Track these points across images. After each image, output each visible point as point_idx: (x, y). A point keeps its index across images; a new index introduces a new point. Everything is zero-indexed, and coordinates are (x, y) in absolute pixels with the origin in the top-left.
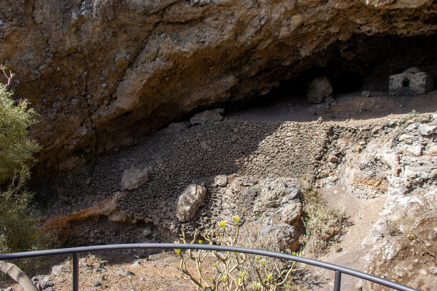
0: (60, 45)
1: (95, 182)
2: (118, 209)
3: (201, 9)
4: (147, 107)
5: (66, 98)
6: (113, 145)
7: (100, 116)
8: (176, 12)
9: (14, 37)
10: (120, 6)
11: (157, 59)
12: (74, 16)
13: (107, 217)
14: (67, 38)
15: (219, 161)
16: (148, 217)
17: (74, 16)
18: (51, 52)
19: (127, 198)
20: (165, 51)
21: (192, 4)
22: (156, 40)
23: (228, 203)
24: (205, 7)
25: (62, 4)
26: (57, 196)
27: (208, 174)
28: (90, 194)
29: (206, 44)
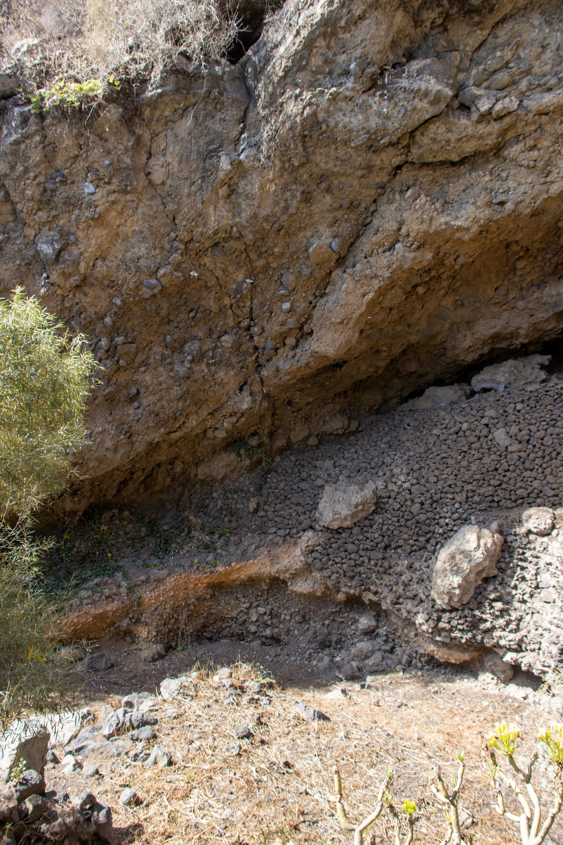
0: (197, 226)
1: (266, 507)
2: (308, 568)
3: (495, 127)
4: (378, 352)
5: (210, 332)
6: (307, 432)
7: (278, 370)
8: (439, 138)
9: (114, 214)
10: (315, 135)
11: (398, 246)
12: (225, 164)
13: (284, 582)
14: (211, 210)
15: (534, 474)
16: (369, 590)
17: (225, 164)
18: (181, 241)
19: (327, 546)
20: (415, 227)
21: (475, 116)
22: (395, 205)
23: (554, 575)
24: (507, 120)
25: (202, 142)
26: (189, 532)
27: (509, 504)
28: (254, 531)
29: (509, 206)
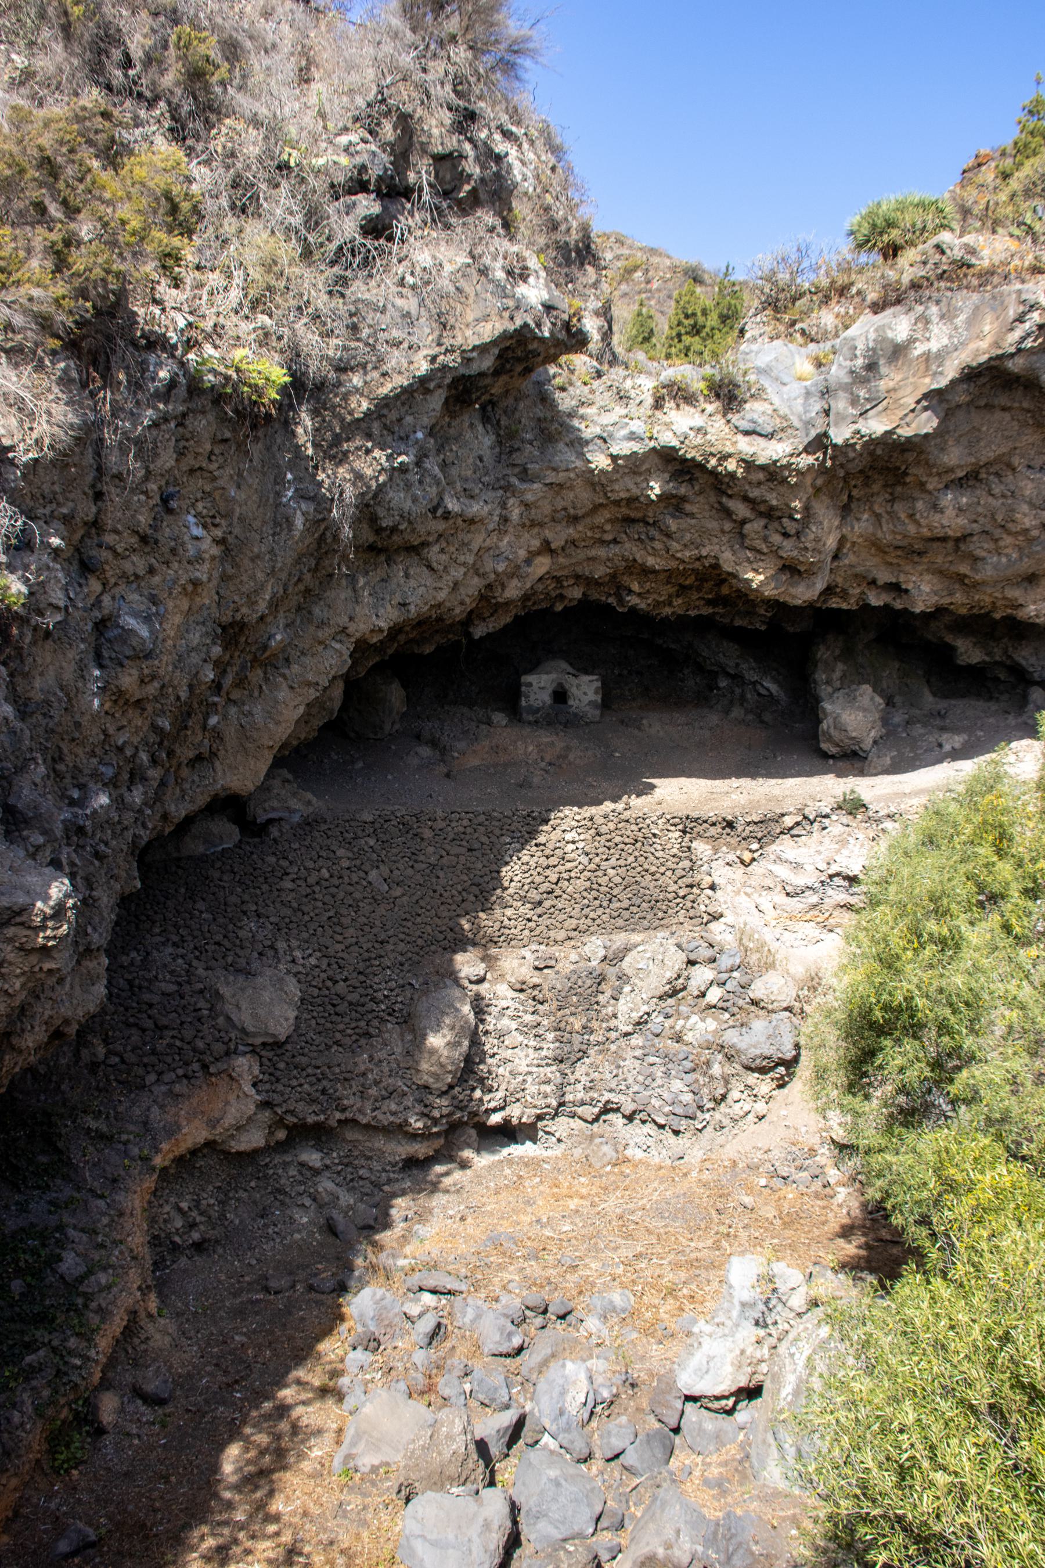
23: (513, 1018)
